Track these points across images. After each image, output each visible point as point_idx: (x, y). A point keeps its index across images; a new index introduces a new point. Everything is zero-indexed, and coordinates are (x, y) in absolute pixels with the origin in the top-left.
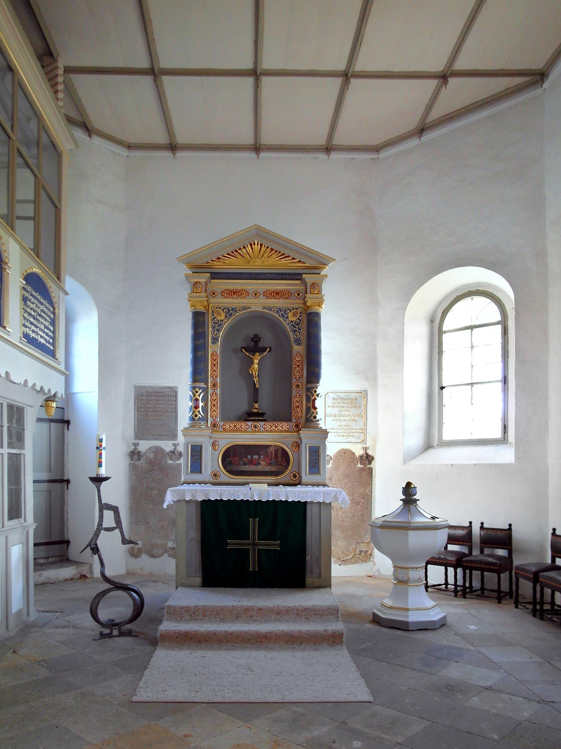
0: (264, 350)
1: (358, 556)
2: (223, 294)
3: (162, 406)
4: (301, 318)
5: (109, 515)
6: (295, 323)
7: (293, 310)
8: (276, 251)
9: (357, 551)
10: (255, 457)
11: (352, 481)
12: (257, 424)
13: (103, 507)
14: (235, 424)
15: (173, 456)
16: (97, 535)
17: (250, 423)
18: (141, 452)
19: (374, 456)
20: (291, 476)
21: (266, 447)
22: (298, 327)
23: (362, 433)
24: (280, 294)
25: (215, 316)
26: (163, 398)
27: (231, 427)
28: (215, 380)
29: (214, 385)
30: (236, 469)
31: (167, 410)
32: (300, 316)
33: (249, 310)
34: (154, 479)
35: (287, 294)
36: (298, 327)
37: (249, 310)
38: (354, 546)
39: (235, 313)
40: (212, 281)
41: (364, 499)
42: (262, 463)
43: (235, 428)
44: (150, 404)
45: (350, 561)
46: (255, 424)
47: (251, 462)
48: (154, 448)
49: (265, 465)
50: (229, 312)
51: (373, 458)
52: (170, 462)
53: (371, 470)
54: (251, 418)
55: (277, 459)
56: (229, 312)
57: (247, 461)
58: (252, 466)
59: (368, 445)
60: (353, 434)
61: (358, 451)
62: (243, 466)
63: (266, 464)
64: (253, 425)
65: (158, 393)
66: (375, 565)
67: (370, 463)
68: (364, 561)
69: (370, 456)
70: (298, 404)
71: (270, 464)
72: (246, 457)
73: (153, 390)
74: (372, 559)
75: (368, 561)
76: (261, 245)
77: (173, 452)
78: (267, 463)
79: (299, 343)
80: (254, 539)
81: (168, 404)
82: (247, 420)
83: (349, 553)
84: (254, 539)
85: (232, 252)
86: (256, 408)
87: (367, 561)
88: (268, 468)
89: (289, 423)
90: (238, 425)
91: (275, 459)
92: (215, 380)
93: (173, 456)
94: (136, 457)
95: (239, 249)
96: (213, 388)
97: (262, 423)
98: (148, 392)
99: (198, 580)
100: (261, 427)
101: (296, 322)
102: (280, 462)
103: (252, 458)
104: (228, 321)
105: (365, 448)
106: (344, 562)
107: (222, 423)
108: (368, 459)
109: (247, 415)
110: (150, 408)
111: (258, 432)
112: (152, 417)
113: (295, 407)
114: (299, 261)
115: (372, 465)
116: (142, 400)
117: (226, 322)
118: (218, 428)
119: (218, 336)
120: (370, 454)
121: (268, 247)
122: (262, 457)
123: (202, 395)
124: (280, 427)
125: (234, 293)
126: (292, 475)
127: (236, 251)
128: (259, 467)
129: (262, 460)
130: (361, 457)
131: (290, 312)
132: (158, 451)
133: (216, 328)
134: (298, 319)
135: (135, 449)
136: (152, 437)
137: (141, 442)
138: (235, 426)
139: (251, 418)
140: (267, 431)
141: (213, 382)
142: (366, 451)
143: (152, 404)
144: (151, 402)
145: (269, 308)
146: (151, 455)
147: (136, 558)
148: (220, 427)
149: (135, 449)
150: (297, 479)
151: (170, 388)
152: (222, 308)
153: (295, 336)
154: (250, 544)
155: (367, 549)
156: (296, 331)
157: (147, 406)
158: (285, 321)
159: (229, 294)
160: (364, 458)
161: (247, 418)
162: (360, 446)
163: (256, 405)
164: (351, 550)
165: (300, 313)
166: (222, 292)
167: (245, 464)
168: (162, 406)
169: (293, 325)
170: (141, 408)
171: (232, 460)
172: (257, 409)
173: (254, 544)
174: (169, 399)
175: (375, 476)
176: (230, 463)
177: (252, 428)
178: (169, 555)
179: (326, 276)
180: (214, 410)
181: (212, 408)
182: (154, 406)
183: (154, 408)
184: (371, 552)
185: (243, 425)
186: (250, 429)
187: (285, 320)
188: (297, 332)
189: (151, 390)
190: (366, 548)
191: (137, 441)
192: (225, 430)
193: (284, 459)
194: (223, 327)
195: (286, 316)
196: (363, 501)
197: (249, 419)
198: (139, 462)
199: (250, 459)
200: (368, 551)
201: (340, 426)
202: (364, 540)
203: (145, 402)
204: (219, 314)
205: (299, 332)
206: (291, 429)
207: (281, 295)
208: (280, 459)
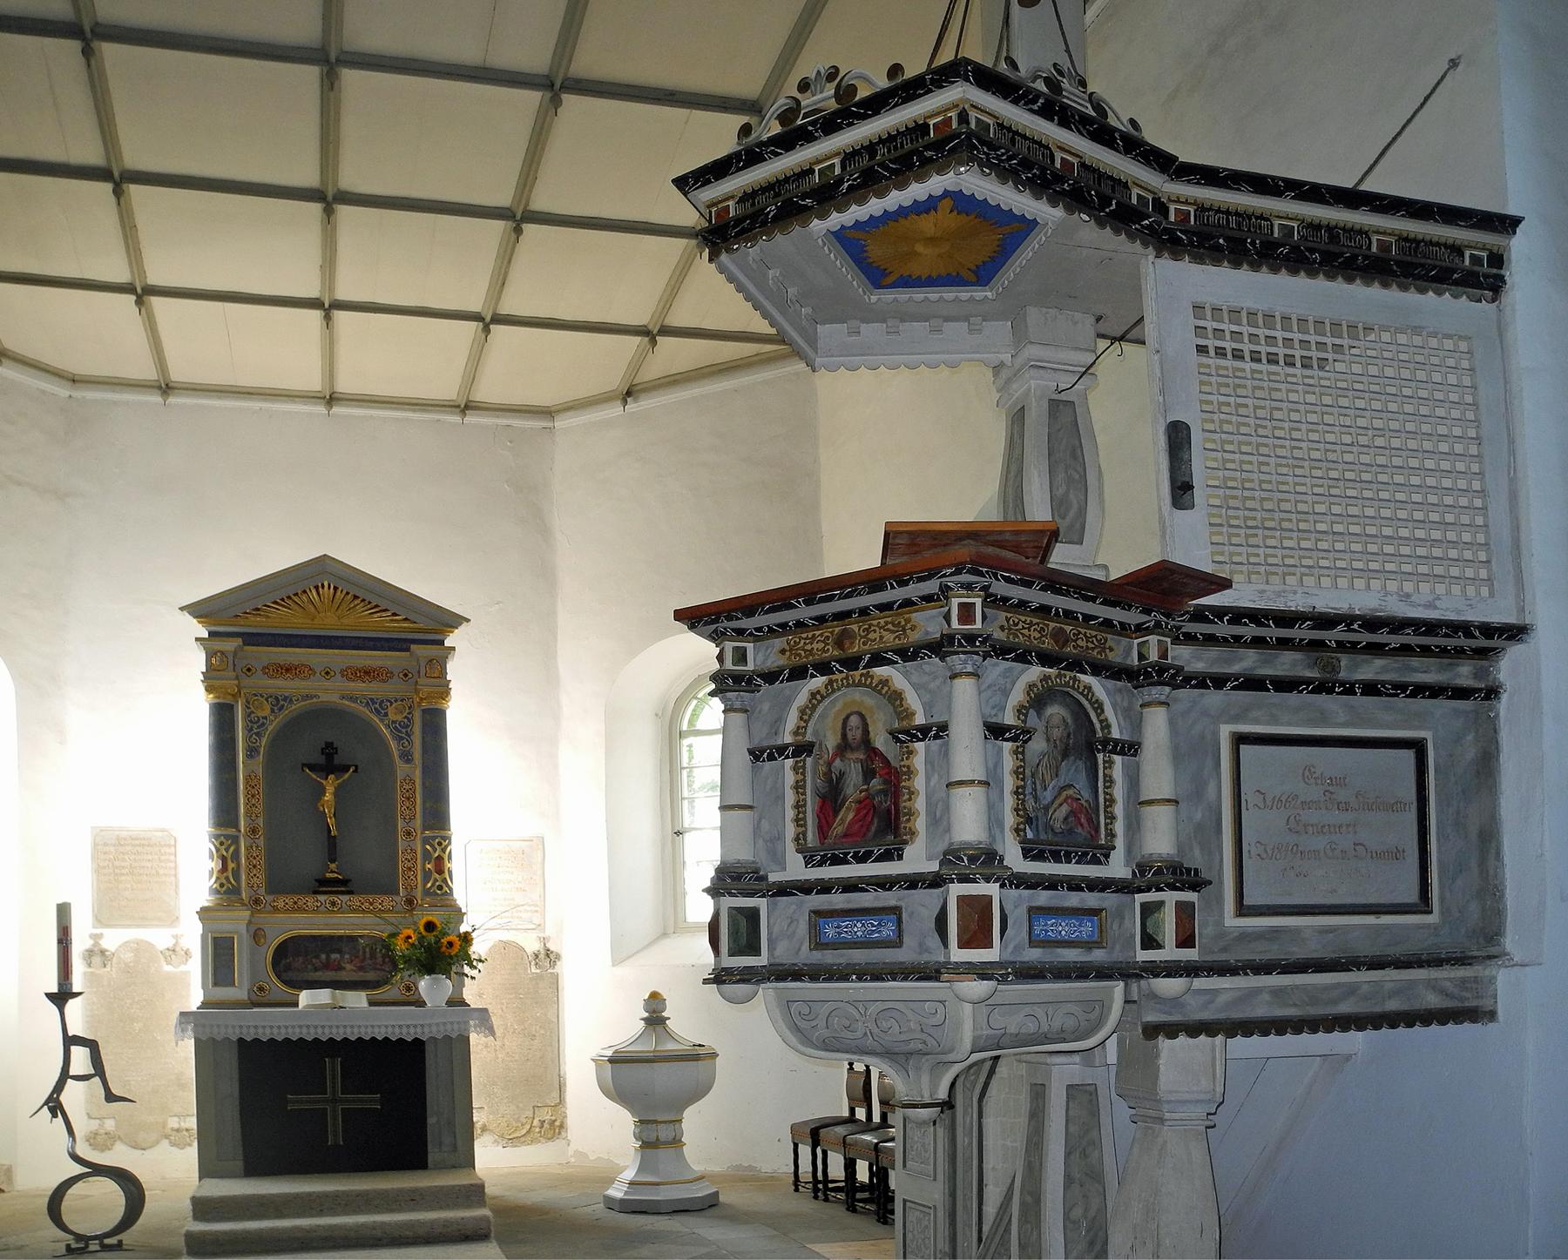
0: (345, 769)
2: (267, 671)
3: (149, 864)
4: (410, 716)
6: (399, 725)
7: (396, 701)
8: (363, 600)
10: (335, 956)
12: (336, 899)
14: (296, 900)
16: (59, 1087)
17: (322, 898)
19: (559, 952)
21: (352, 939)
22: (407, 732)
23: (536, 911)
25: (253, 709)
26: (149, 848)
30: (299, 979)
31: (158, 873)
32: (409, 713)
33: (315, 700)
34: (136, 1000)
36: (407, 732)
37: (315, 700)
40: (246, 648)
42: (348, 967)
44: (124, 860)
46: (331, 899)
47: (327, 966)
48: (134, 943)
49: (352, 970)
51: (558, 957)
53: (556, 978)
54: (325, 889)
56: (278, 702)
59: (547, 934)
60: (520, 914)
61: (531, 945)
65: (137, 839)
67: (553, 964)
69: (552, 952)
70: (410, 865)
71: (361, 968)
72: (317, 957)
73: (130, 833)
76: (336, 588)
79: (408, 759)
80: (334, 1092)
81: (160, 861)
82: (316, 892)
84: (334, 1092)
85: (283, 600)
86: (332, 872)
89: (395, 898)
95: (294, 595)
97: (345, 898)
98: (118, 838)
99: (240, 1164)
102: (381, 965)
103: (328, 957)
107: (270, 898)
108: (548, 957)
109: (317, 884)
111: (337, 912)
114: (406, 619)
115: (557, 969)
118: (262, 905)
119: (258, 744)
120: (552, 949)
121: (348, 593)
122: (347, 956)
123: (232, 849)
127: (289, 597)
128: (344, 973)
131: (391, 705)
133: (255, 731)
134: (406, 717)
138: (295, 903)
139: (325, 889)
140: (354, 911)
142: (545, 944)
145: (352, 699)
148: (267, 904)
150: (412, 992)
156: (402, 738)
157: (117, 863)
158: (382, 721)
160: (542, 956)
161: (317, 889)
162: (534, 935)
163: (333, 866)
165: (409, 708)
166: (264, 668)
167: (316, 970)
168: (149, 864)
169: (396, 728)
171: (290, 963)
172: (335, 872)
174: (162, 851)
175: (563, 988)
176: (288, 968)
177: (327, 905)
179: (453, 649)
180: (255, 875)
183: (131, 867)
186: (322, 908)
188: (405, 741)
189: (124, 834)
192: (276, 910)
196: (542, 1032)
197: (321, 889)
199: (324, 961)
204: (261, 707)
206: (399, 908)
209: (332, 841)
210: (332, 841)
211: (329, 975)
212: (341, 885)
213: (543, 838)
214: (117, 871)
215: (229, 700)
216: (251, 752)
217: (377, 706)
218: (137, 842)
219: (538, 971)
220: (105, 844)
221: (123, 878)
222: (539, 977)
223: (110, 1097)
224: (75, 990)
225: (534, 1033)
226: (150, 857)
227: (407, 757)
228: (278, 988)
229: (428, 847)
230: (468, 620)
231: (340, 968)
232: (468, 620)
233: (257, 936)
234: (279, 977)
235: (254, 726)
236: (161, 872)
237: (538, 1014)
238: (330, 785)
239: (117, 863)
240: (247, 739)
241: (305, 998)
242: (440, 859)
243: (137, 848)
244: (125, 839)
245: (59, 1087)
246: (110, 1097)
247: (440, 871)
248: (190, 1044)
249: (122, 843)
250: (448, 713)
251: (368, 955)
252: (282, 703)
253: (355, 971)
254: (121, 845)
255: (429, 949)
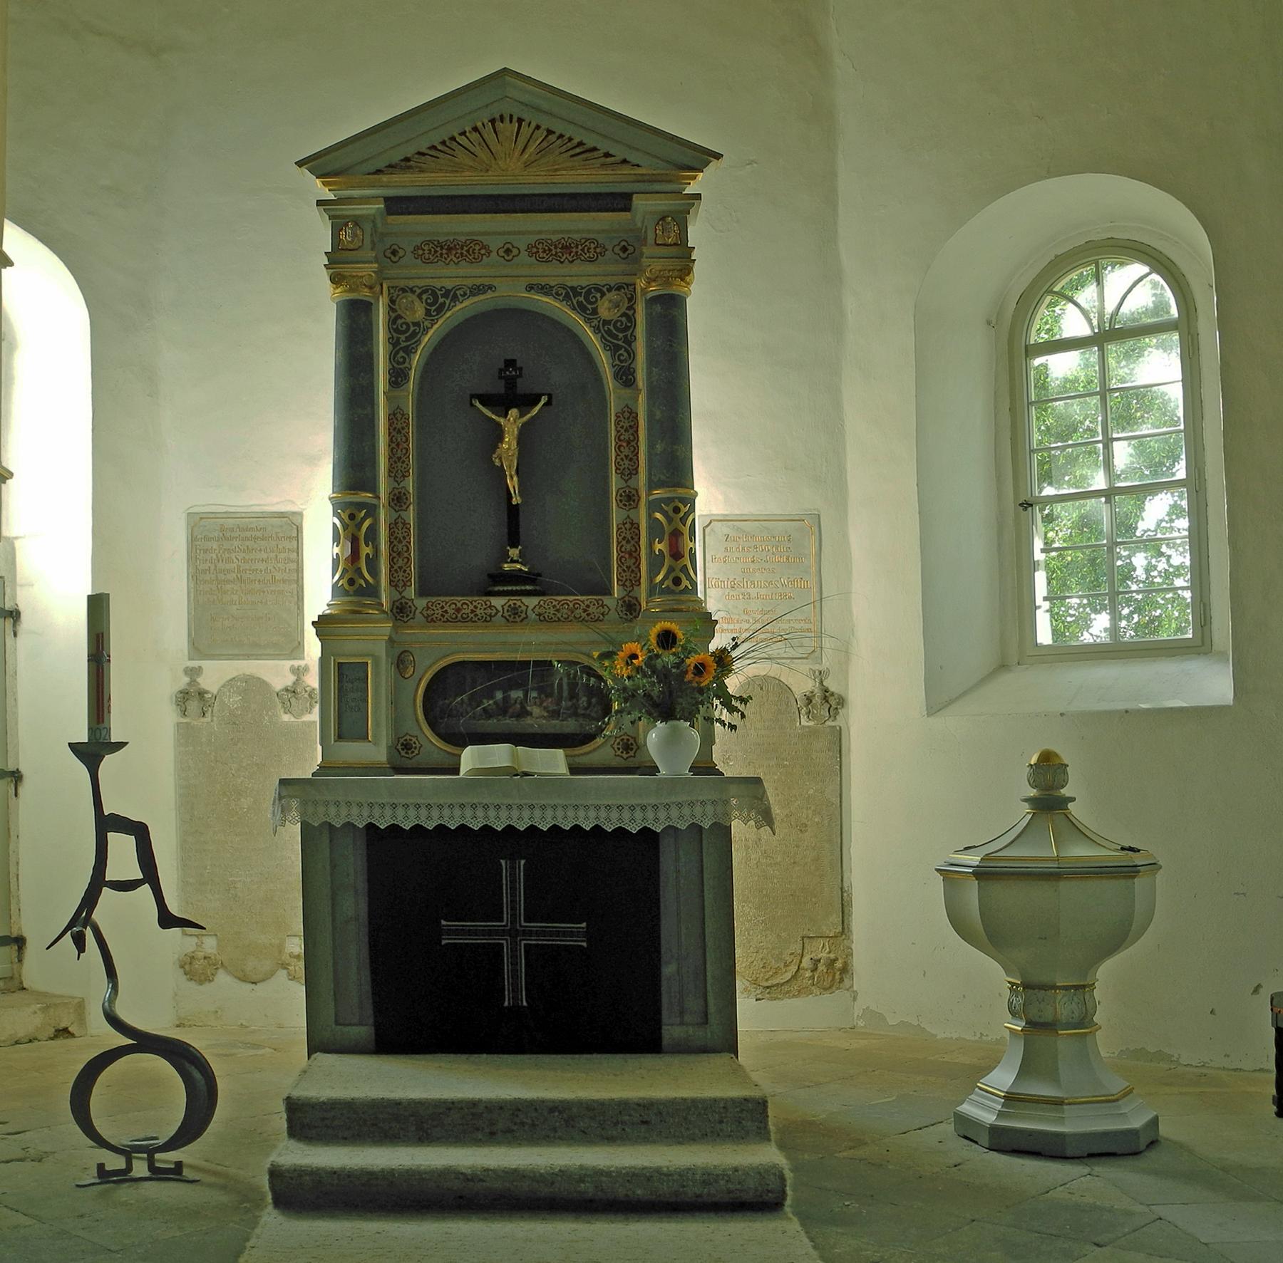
0: (534, 400)
1: (808, 974)
2: (420, 252)
3: (262, 566)
4: (630, 313)
5: (122, 847)
6: (615, 326)
8: (561, 136)
9: (806, 962)
10: (516, 694)
11: (785, 766)
13: (106, 824)
15: (293, 700)
16: (90, 900)
17: (498, 602)
18: (207, 692)
20: (616, 746)
21: (544, 667)
22: (626, 337)
23: (809, 630)
24: (574, 250)
25: (399, 312)
27: (446, 612)
28: (400, 486)
29: (398, 500)
33: (489, 295)
35: (592, 250)
36: (626, 337)
38: (797, 947)
39: (452, 304)
40: (391, 218)
41: (819, 813)
42: (536, 711)
43: (459, 616)
45: (786, 988)
47: (503, 709)
50: (436, 301)
51: (842, 701)
52: (287, 718)
55: (574, 701)
56: (437, 301)
57: (494, 707)
58: (507, 721)
59: (826, 664)
61: (802, 684)
62: (482, 721)
63: (546, 714)
64: (506, 608)
66: (855, 999)
68: (825, 989)
69: (832, 694)
71: (555, 714)
74: (847, 982)
75: (838, 988)
76: (520, 121)
77: (292, 691)
78: (548, 712)
83: (782, 966)
85: (443, 143)
86: (513, 561)
87: (834, 988)
88: (555, 726)
90: (465, 606)
91: (570, 700)
92: (400, 486)
93: (293, 700)
94: (193, 705)
95: (461, 134)
96: (397, 508)
97: (532, 602)
100: (530, 612)
101: (619, 324)
104: (432, 326)
105: (817, 673)
106: (771, 991)
107: (421, 603)
110: (229, 571)
112: (235, 597)
113: (623, 554)
116: (206, 551)
117: (428, 328)
119: (406, 365)
120: (832, 689)
121: (538, 127)
124: (581, 611)
125: (449, 249)
126: (619, 744)
127: (453, 139)
128: (529, 721)
129: (535, 704)
130: (809, 700)
132: (252, 687)
133: (403, 344)
134: (624, 315)
135: (193, 682)
136: (236, 652)
137: (206, 664)
141: (396, 491)
142: (821, 683)
143: (235, 560)
144: (233, 556)
146: (234, 700)
147: (201, 983)
149: (193, 682)
151: (282, 515)
152: (418, 291)
153: (617, 362)
154: (503, 933)
155: (832, 956)
156: (617, 348)
158: (587, 321)
159: (436, 252)
160: (817, 700)
161: (490, 589)
162: (805, 667)
163: (514, 552)
164: (789, 959)
166: (417, 248)
167: (487, 714)
168: (262, 566)
169: (609, 332)
170: (204, 572)
173: (514, 933)
178: (289, 974)
181: (395, 560)
182: (239, 567)
184: (846, 965)
185: (479, 606)
187: (589, 319)
188: (622, 352)
190: (830, 952)
191: (195, 664)
192: (430, 620)
193: (594, 700)
194: (419, 341)
195: (589, 307)
197: (496, 589)
198: (205, 720)
200: (836, 960)
201: (746, 612)
202: (824, 928)
203: (215, 557)
205: (626, 350)
207: (577, 252)
208: (583, 701)
209: (513, 512)
210: (513, 512)
211: (509, 723)
212: (531, 582)
213: (819, 515)
214: (222, 577)
215: (365, 294)
216: (398, 377)
217: (581, 299)
218: (248, 534)
219: (811, 723)
220: (206, 538)
221: (229, 587)
222: (813, 733)
223: (167, 919)
224: (114, 738)
225: (805, 821)
226: (265, 556)
227: (626, 376)
228: (431, 744)
229: (658, 515)
230: (718, 156)
231: (524, 713)
232: (718, 156)
233: (401, 662)
234: (433, 725)
235: (403, 338)
236: (279, 576)
237: (811, 792)
238: (512, 423)
239: (221, 566)
240: (392, 357)
241: (469, 758)
242: (676, 535)
243: (248, 543)
244: (232, 530)
245: (90, 900)
246: (167, 919)
247: (676, 555)
248: (294, 831)
249: (228, 535)
250: (690, 302)
251: (565, 694)
252: (441, 300)
253: (544, 718)
254: (227, 539)
255: (664, 675)
